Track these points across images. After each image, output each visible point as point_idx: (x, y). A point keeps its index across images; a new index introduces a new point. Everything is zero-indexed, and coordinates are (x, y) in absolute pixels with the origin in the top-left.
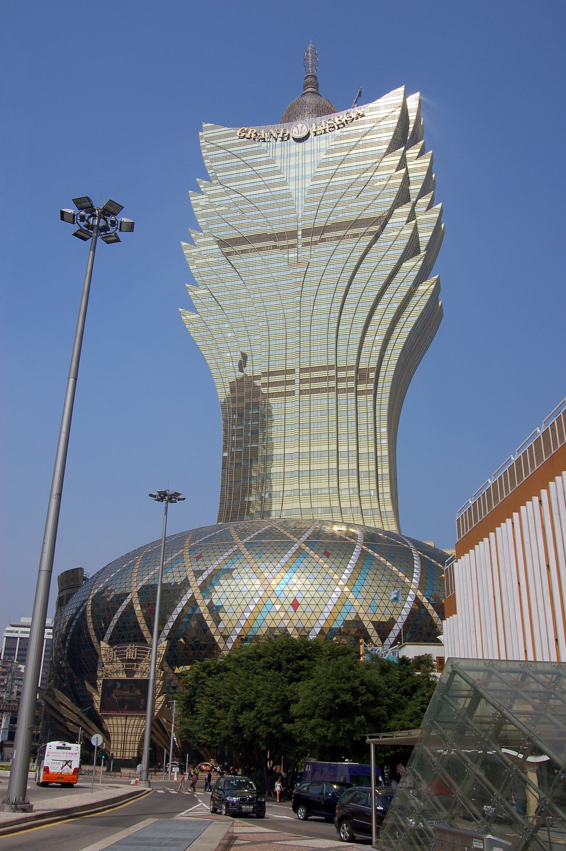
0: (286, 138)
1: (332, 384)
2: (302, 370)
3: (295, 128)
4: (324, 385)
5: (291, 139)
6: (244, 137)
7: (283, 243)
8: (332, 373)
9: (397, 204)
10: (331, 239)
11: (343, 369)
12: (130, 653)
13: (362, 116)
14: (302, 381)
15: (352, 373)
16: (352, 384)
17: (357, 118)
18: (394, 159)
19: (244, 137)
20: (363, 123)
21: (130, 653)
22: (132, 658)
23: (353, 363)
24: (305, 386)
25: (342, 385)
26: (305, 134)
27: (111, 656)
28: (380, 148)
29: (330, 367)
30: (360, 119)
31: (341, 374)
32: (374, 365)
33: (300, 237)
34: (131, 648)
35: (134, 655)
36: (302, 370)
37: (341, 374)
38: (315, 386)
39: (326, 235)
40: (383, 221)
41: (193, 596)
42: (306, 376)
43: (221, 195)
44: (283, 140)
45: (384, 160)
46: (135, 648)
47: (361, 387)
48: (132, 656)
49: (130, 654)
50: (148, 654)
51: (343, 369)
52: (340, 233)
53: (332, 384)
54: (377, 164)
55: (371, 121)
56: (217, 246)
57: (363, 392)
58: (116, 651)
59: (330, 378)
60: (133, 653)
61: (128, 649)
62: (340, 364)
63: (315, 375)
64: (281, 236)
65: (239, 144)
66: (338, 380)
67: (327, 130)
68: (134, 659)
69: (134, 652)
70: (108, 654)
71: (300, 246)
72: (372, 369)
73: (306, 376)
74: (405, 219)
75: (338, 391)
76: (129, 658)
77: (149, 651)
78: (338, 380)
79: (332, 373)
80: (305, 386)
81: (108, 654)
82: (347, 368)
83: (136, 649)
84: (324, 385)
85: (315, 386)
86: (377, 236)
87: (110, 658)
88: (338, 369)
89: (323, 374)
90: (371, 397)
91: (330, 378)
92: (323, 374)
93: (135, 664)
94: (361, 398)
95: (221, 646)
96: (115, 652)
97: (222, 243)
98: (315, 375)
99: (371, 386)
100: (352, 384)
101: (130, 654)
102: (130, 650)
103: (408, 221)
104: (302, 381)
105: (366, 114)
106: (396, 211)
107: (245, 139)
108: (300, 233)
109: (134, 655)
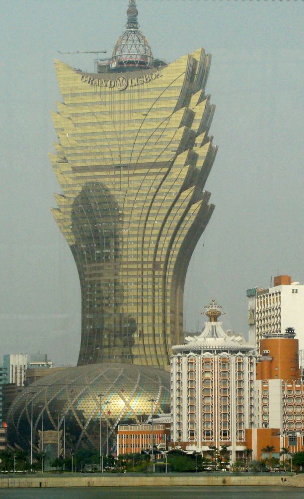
3: (118, 81)
9: (179, 151)
15: (151, 266)
18: (180, 114)
23: (151, 259)
26: (123, 87)
30: (160, 79)
31: (145, 266)
32: (163, 259)
39: (138, 171)
40: (170, 165)
45: (174, 115)
47: (157, 273)
52: (146, 171)
56: (71, 169)
62: (145, 260)
72: (161, 262)
74: (183, 163)
82: (148, 262)
86: (167, 174)
88: (143, 263)
89: (135, 266)
90: (161, 280)
91: (138, 269)
92: (135, 266)
95: (82, 428)
98: (131, 266)
99: (161, 273)
100: (150, 273)
106: (178, 156)
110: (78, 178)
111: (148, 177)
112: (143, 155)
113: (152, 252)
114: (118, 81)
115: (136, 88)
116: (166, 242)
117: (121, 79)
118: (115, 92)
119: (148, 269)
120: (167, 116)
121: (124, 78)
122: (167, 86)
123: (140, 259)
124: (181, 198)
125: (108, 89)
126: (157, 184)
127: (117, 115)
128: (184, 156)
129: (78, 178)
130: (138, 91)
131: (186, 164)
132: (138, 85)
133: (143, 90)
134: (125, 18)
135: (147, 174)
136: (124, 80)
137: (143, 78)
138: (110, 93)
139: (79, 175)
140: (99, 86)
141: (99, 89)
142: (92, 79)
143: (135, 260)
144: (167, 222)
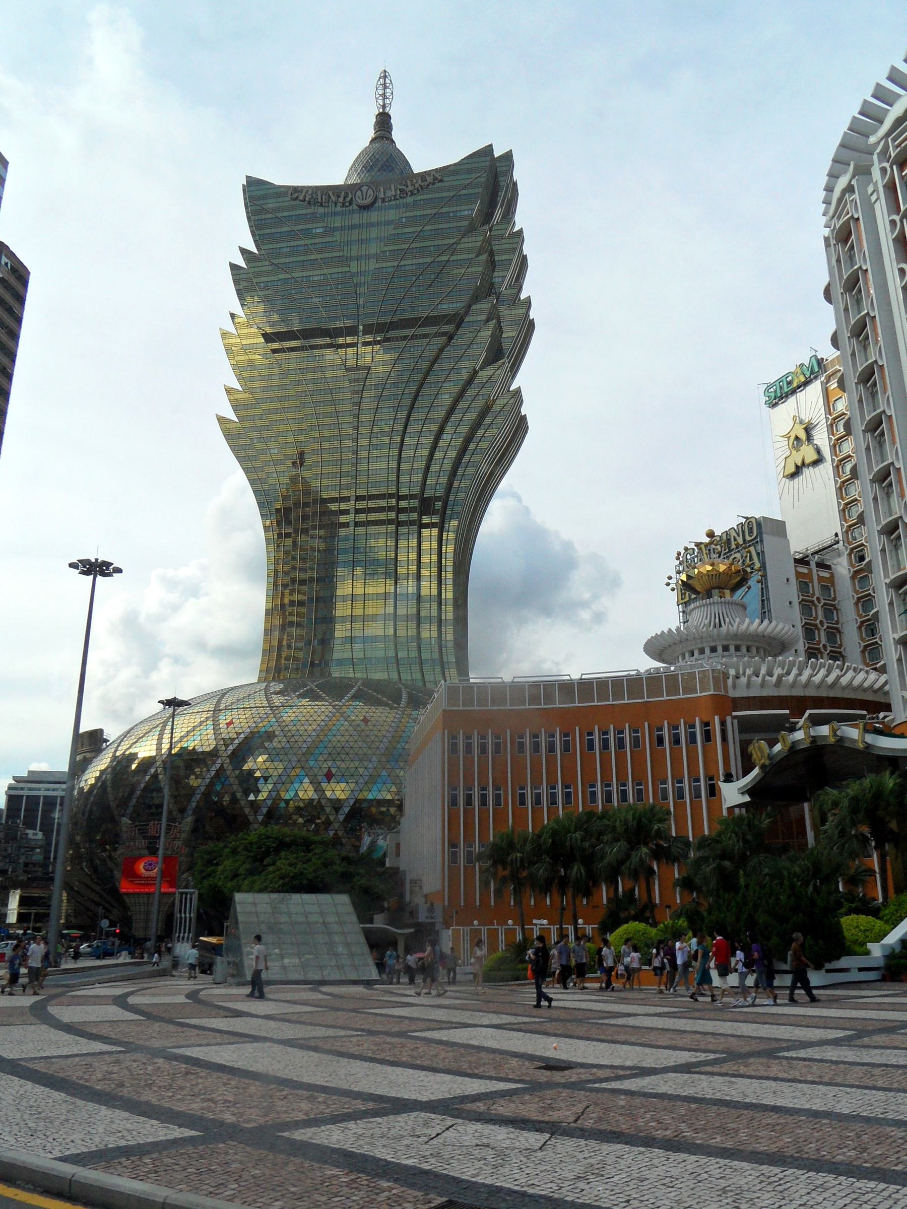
0: (347, 204)
1: (392, 515)
2: (358, 498)
4: (382, 516)
5: (355, 207)
6: (296, 199)
7: (341, 340)
8: (393, 502)
10: (397, 339)
11: (404, 497)
13: (441, 181)
14: (358, 511)
15: (415, 503)
16: (414, 516)
17: (434, 184)
18: (474, 241)
19: (296, 199)
20: (441, 190)
23: (416, 491)
24: (362, 517)
25: (403, 517)
28: (458, 224)
29: (390, 496)
30: (437, 185)
31: (403, 504)
32: (440, 493)
33: (361, 333)
36: (358, 498)
37: (403, 504)
38: (373, 517)
39: (392, 334)
40: (458, 320)
41: (222, 767)
42: (362, 505)
43: (268, 274)
44: (343, 206)
45: (464, 240)
47: (426, 520)
51: (404, 497)
53: (392, 515)
54: (454, 246)
55: (449, 189)
56: (262, 340)
57: (427, 526)
59: (390, 509)
62: (403, 492)
63: (373, 504)
64: (338, 332)
65: (288, 209)
66: (400, 511)
67: (398, 197)
71: (360, 346)
72: (438, 499)
73: (362, 505)
74: (484, 317)
75: (399, 524)
78: (400, 511)
79: (393, 502)
80: (362, 517)
82: (412, 497)
84: (382, 516)
85: (373, 517)
86: (451, 338)
88: (400, 498)
89: (383, 503)
90: (435, 532)
91: (390, 509)
92: (383, 503)
94: (425, 532)
97: (268, 338)
98: (373, 504)
103: (488, 321)
104: (358, 511)
105: (445, 179)
106: (474, 307)
107: (297, 202)
108: (361, 328)
110: (274, 351)
111: (412, 343)
112: (401, 307)
113: (418, 477)
114: (359, 193)
115: (393, 203)
116: (446, 461)
117: (365, 189)
118: (352, 212)
119: (412, 510)
120: (452, 241)
121: (369, 187)
122: (452, 194)
123: (393, 490)
124: (477, 381)
125: (339, 209)
126: (431, 352)
127: (355, 247)
128: (484, 306)
129: (274, 351)
130: (397, 207)
131: (488, 321)
132: (395, 199)
133: (406, 205)
134: (371, 134)
135: (414, 337)
138: (342, 214)
139: (276, 346)
140: (321, 205)
141: (321, 210)
143: (383, 491)
144: (449, 424)
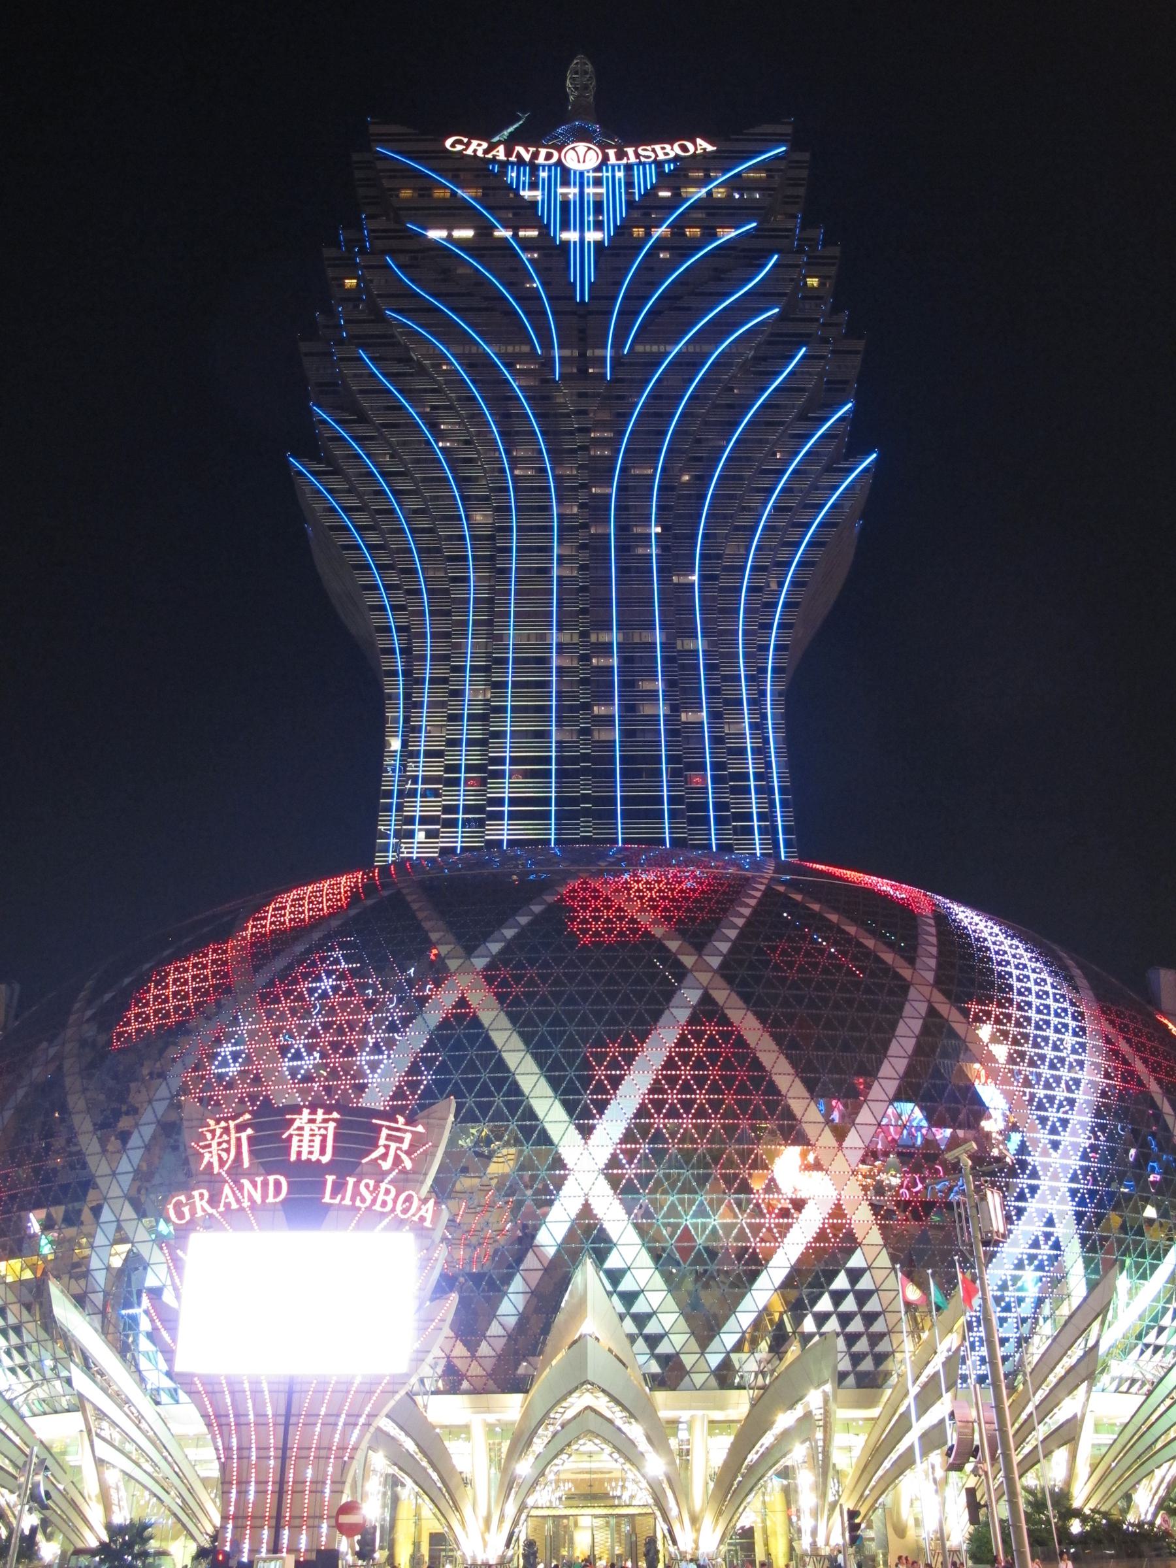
12: (306, 1138)
21: (306, 1138)
22: (314, 1158)
27: (227, 1151)
34: (312, 1121)
35: (323, 1151)
46: (325, 1121)
48: (317, 1149)
49: (305, 1144)
50: (382, 1141)
58: (250, 1131)
60: (318, 1139)
61: (296, 1124)
68: (326, 1159)
69: (324, 1137)
70: (214, 1144)
76: (304, 1157)
77: (385, 1132)
81: (214, 1144)
83: (332, 1125)
87: (224, 1155)
93: (330, 1179)
96: (244, 1136)
101: (305, 1144)
102: (307, 1127)
109: (323, 1151)
136: (591, 152)
137: (654, 150)
142: (485, 145)
